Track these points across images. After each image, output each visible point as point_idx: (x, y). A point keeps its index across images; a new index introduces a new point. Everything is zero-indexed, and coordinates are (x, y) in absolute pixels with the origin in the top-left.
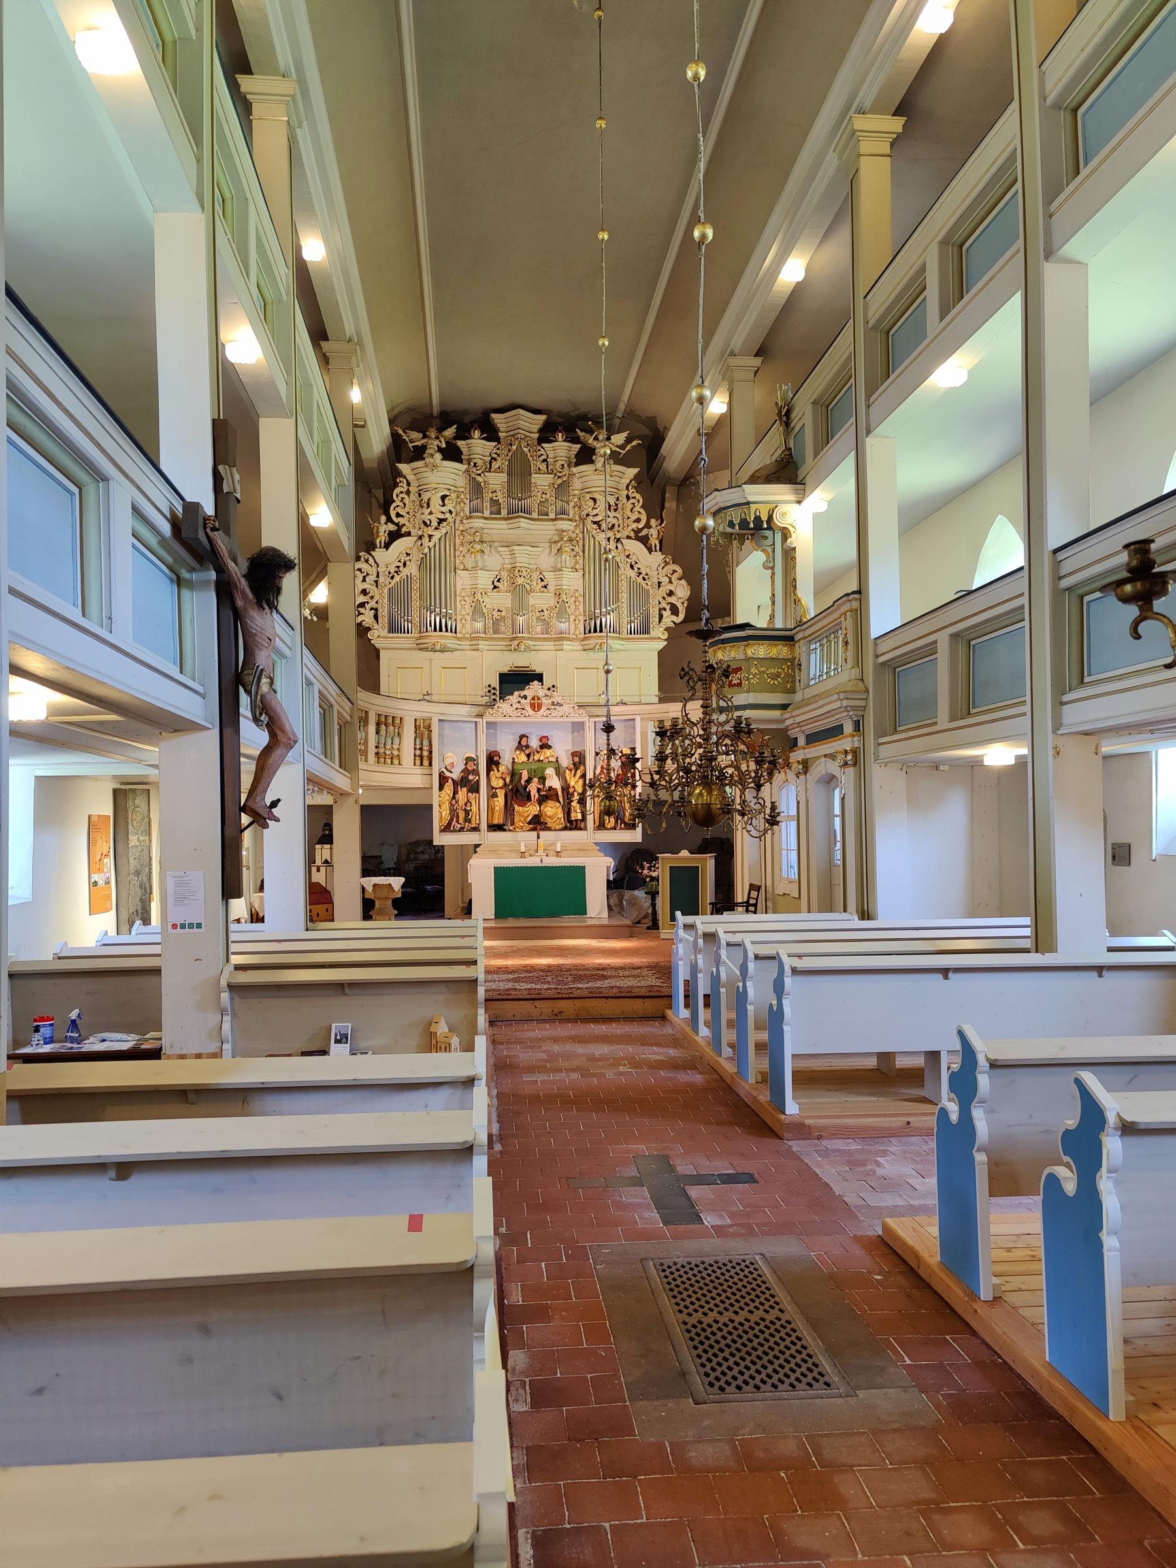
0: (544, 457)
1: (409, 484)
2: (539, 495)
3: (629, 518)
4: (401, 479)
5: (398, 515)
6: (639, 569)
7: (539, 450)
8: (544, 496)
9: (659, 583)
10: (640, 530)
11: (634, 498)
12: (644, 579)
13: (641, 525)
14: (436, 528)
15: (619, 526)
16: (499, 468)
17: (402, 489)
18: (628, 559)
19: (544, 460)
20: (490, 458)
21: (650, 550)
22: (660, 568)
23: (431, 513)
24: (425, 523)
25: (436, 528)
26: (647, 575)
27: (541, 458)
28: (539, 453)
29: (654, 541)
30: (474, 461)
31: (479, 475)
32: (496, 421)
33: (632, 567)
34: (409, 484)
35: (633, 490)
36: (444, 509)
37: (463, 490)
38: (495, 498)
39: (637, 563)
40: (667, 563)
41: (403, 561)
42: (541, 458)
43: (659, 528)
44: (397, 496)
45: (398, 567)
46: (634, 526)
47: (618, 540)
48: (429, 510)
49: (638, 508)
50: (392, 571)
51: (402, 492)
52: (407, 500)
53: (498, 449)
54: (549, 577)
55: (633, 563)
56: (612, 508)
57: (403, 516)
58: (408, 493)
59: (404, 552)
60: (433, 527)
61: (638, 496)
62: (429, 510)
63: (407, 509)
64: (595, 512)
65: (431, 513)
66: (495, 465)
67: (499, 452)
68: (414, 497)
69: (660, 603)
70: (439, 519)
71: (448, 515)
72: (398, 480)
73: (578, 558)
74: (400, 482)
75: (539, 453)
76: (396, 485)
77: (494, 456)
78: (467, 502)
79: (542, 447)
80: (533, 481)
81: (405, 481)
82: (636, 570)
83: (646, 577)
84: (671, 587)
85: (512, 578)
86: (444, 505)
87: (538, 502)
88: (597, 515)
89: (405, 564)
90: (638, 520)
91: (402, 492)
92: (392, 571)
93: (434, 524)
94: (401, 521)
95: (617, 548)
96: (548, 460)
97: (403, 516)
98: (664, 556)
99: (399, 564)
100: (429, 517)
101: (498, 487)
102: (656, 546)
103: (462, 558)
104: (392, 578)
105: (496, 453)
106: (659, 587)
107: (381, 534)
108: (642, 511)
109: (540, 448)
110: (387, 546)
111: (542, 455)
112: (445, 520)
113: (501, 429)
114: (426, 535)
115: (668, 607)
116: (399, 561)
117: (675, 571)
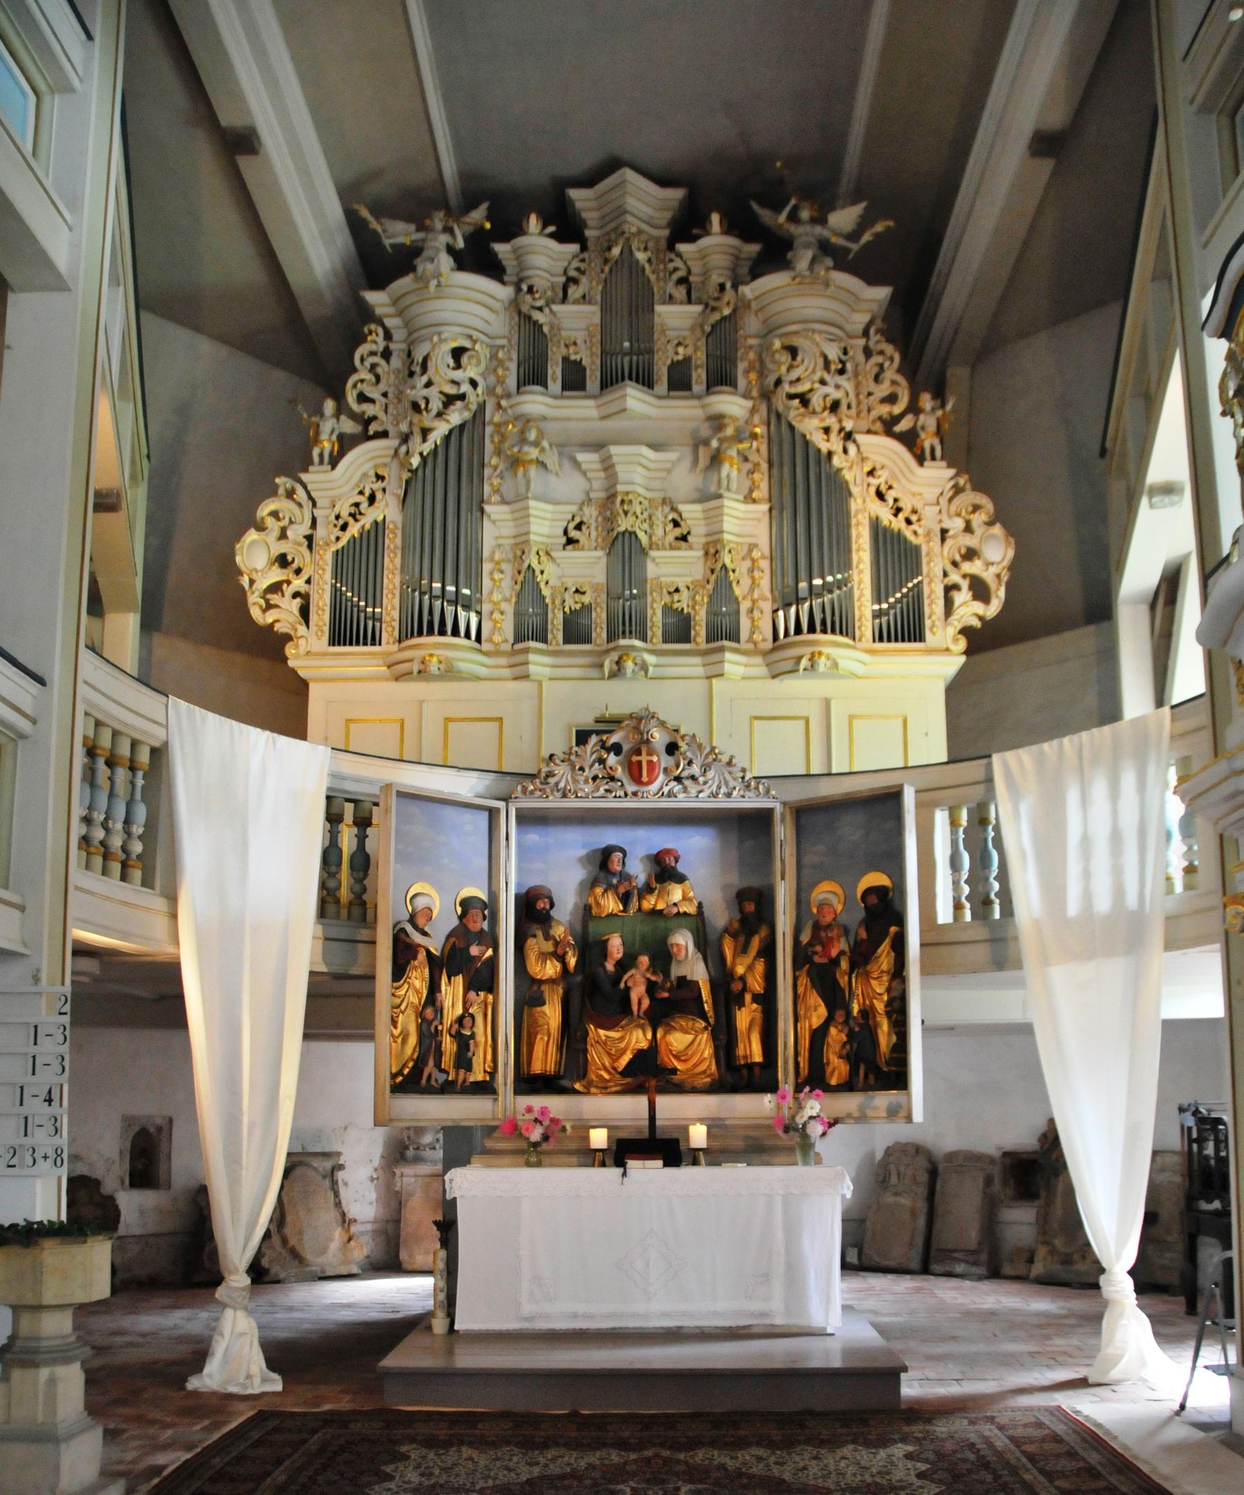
0: (682, 273)
1: (388, 336)
2: (670, 348)
3: (870, 394)
4: (373, 327)
5: (362, 398)
6: (896, 500)
7: (671, 261)
8: (681, 350)
9: (944, 532)
10: (896, 419)
11: (881, 353)
12: (908, 522)
13: (897, 409)
14: (439, 415)
15: (849, 407)
16: (584, 297)
17: (374, 347)
18: (871, 480)
19: (683, 281)
20: (563, 279)
21: (920, 460)
22: (943, 501)
23: (429, 384)
24: (416, 407)
25: (439, 415)
26: (914, 512)
27: (675, 277)
28: (671, 266)
29: (928, 441)
30: (530, 282)
31: (540, 309)
32: (578, 205)
33: (880, 496)
34: (388, 336)
35: (878, 337)
36: (458, 375)
37: (504, 342)
38: (573, 358)
39: (890, 487)
40: (958, 490)
41: (367, 492)
42: (675, 277)
43: (939, 413)
44: (362, 360)
45: (357, 505)
46: (884, 410)
47: (849, 436)
48: (425, 379)
49: (890, 374)
50: (345, 514)
51: (373, 353)
52: (383, 368)
53: (583, 260)
54: (692, 513)
55: (883, 488)
56: (833, 367)
57: (372, 401)
58: (387, 354)
59: (372, 473)
60: (434, 412)
61: (889, 349)
62: (425, 379)
63: (382, 387)
64: (794, 374)
65: (429, 384)
66: (574, 292)
67: (582, 266)
68: (396, 362)
69: (945, 574)
70: (446, 395)
71: (466, 388)
72: (366, 330)
73: (756, 476)
74: (370, 333)
75: (671, 266)
76: (362, 339)
77: (573, 273)
78: (513, 366)
79: (679, 255)
80: (657, 320)
81: (380, 331)
82: (891, 502)
83: (914, 518)
84: (970, 541)
85: (609, 521)
86: (458, 366)
87: (669, 362)
88: (798, 380)
89: (372, 499)
90: (891, 399)
91: (373, 353)
92: (345, 515)
93: (436, 405)
94: (369, 410)
95: (845, 451)
96: (691, 279)
97: (372, 401)
98: (952, 472)
99: (359, 499)
100: (425, 392)
101: (580, 337)
102: (933, 450)
103: (496, 481)
104: (344, 527)
105: (578, 269)
106: (943, 540)
107: (324, 436)
108: (900, 379)
109: (672, 256)
110: (334, 463)
111: (676, 269)
112: (462, 397)
113: (590, 223)
114: (416, 430)
115: (965, 584)
116: (361, 493)
117: (976, 508)
